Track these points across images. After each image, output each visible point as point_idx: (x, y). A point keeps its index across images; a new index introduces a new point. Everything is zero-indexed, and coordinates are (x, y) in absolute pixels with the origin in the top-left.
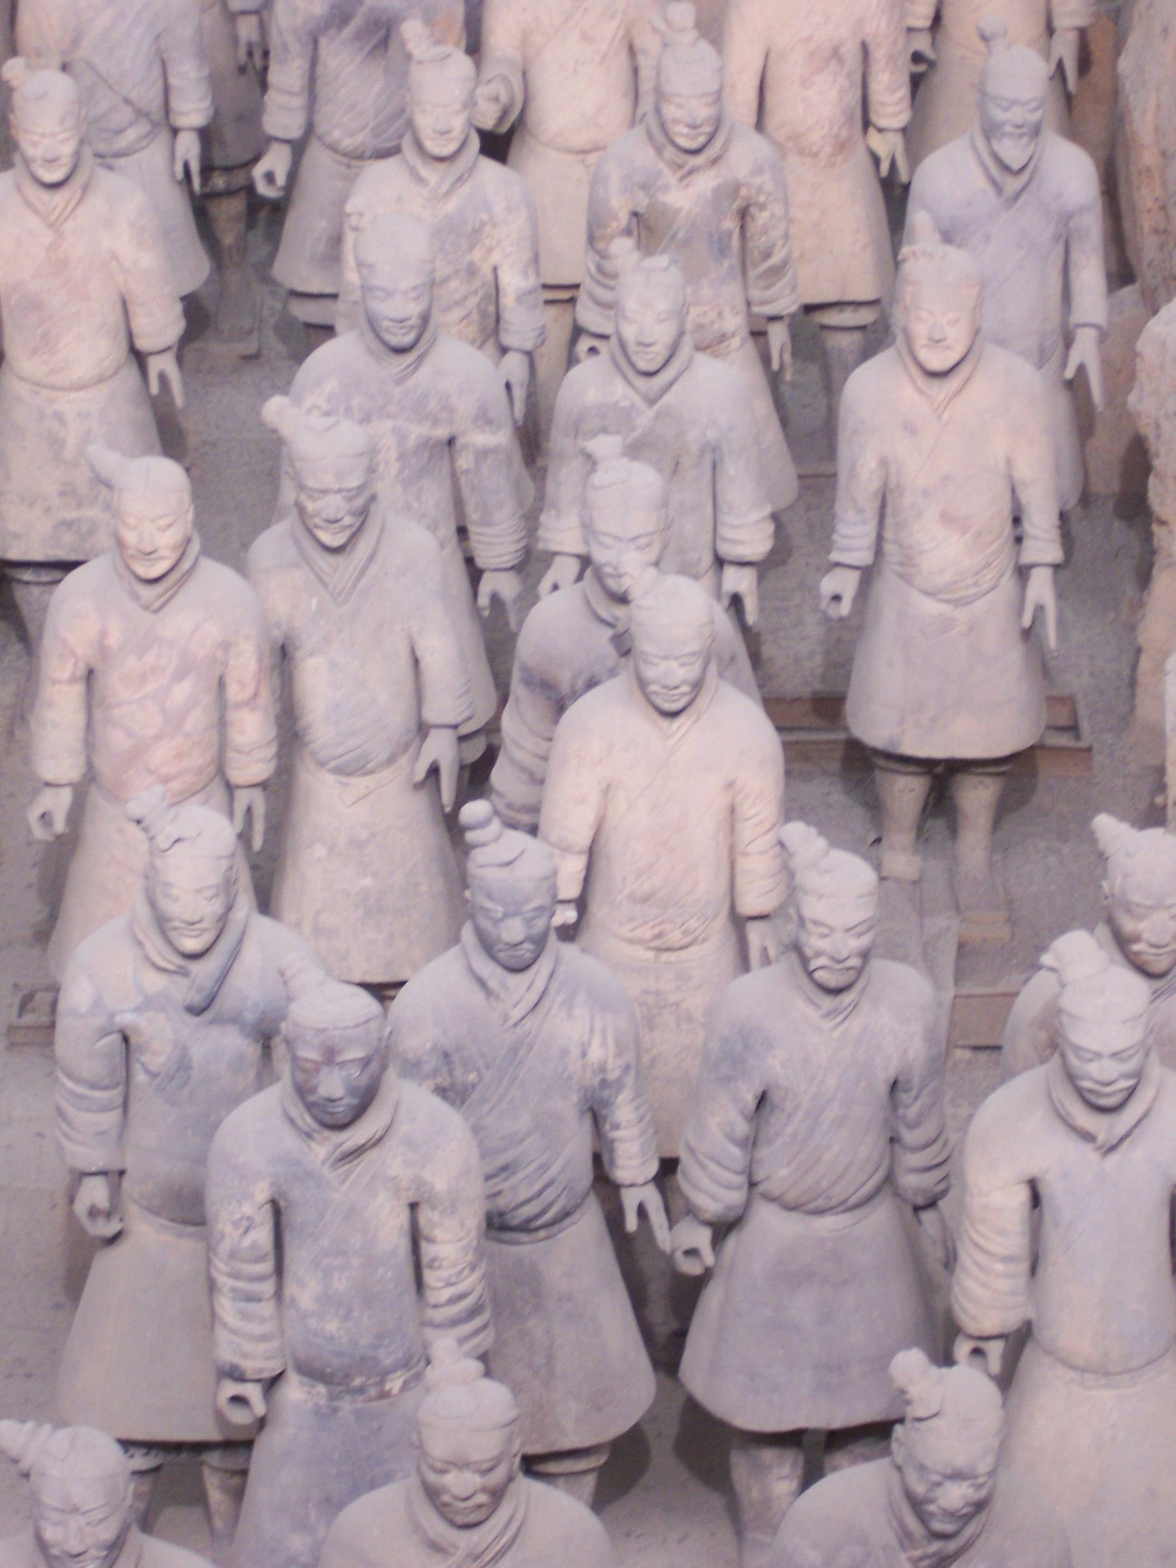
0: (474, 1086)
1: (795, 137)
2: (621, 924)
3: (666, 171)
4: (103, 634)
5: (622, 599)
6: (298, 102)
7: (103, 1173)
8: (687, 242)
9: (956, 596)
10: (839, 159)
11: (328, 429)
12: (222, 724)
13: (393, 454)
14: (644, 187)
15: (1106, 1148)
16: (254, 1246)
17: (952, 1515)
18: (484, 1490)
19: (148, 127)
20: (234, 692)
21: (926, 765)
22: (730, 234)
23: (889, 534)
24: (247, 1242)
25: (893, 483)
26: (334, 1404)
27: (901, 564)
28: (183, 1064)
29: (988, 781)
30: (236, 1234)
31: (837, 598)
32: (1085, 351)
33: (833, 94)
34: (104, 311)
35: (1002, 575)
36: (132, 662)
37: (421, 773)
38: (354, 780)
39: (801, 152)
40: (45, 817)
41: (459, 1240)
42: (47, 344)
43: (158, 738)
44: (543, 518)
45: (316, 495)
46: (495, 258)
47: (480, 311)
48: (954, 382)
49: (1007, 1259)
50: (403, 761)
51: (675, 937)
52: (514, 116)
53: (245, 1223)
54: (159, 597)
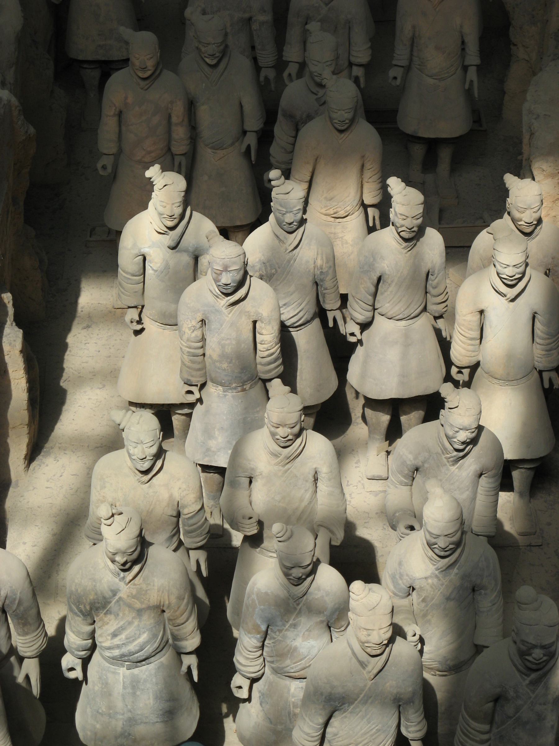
0: (274, 274)
2: (322, 208)
4: (126, 98)
5: (321, 86)
7: (135, 307)
9: (439, 77)
11: (210, 20)
12: (169, 132)
15: (510, 299)
16: (196, 336)
17: (463, 443)
18: (291, 434)
20: (174, 119)
23: (415, 54)
24: (193, 335)
26: (225, 393)
27: (419, 65)
30: (189, 332)
31: (395, 78)
35: (457, 69)
37: (244, 148)
38: (218, 151)
40: (104, 167)
41: (272, 334)
44: (285, 48)
45: (205, 45)
49: (472, 339)
50: (237, 144)
51: (342, 213)
53: (193, 328)
54: (148, 84)
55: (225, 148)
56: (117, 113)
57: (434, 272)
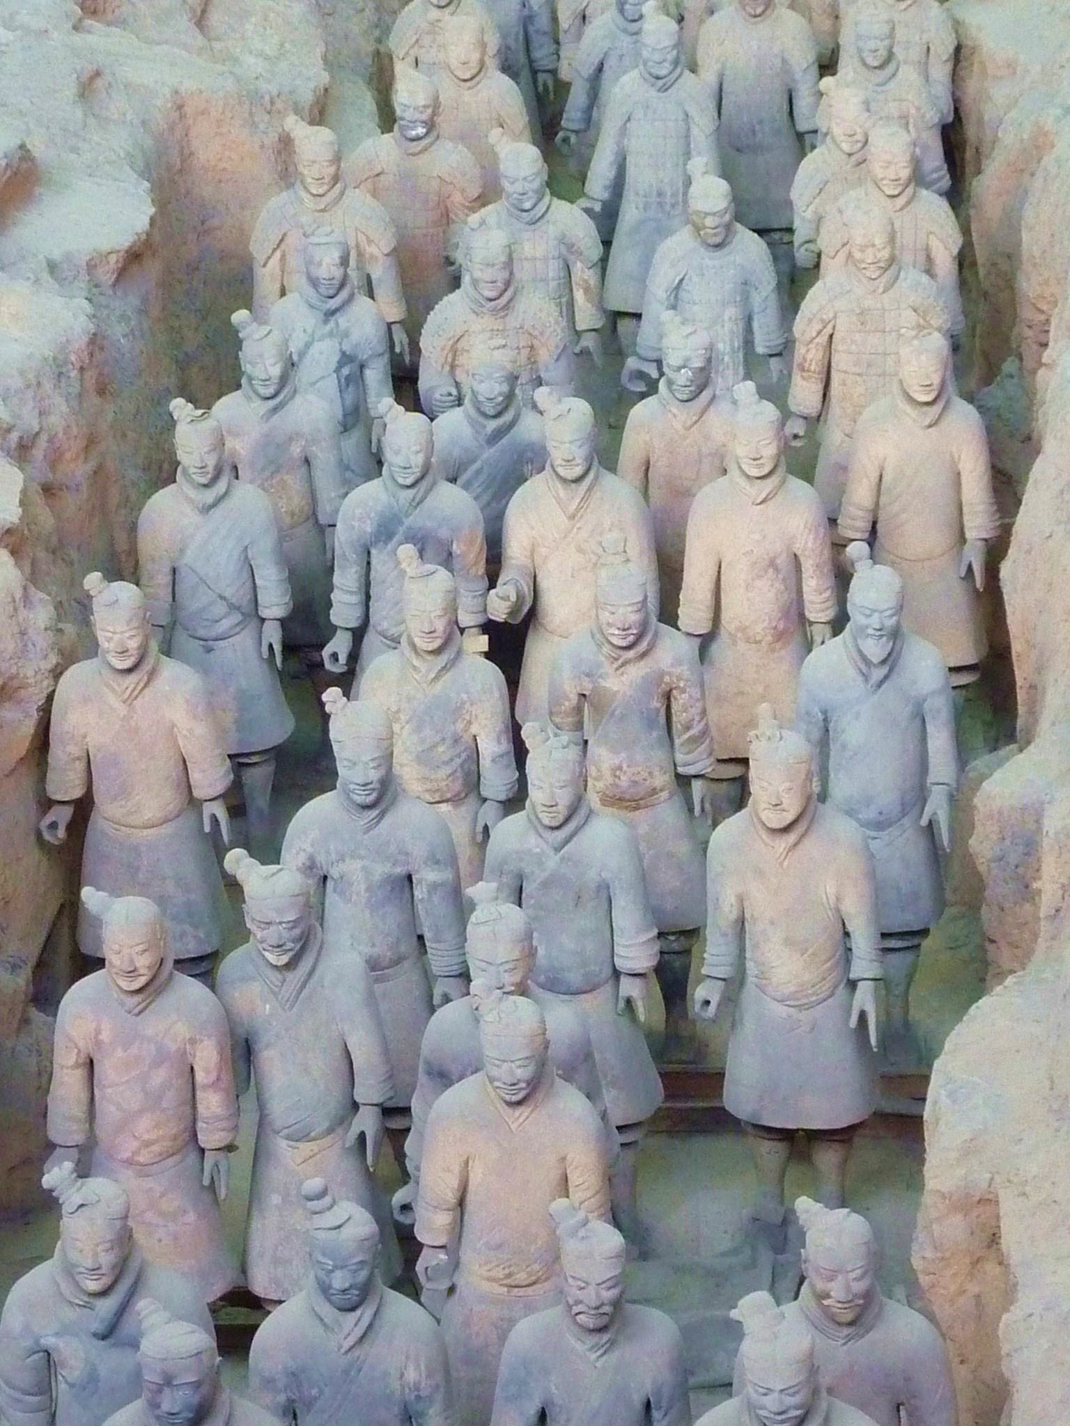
0: (316, 1399)
1: (743, 629)
3: (606, 663)
4: (98, 1032)
6: (355, 599)
8: (623, 718)
10: (778, 646)
11: (273, 874)
13: (363, 887)
14: (588, 675)
19: (240, 617)
20: (200, 1077)
21: (786, 1135)
22: (658, 710)
25: (747, 916)
28: (92, 1379)
29: (837, 1146)
31: (707, 1003)
32: (937, 807)
33: (771, 595)
34: (164, 767)
35: (836, 987)
36: (119, 1053)
39: (748, 641)
42: (124, 792)
43: (141, 1112)
45: (262, 926)
46: (474, 729)
47: (463, 769)
48: (792, 837)
50: (340, 1131)
51: (521, 1277)
52: (526, 609)
54: (139, 1004)
55: (314, 1139)
56: (81, 1061)
57: (659, 1402)
